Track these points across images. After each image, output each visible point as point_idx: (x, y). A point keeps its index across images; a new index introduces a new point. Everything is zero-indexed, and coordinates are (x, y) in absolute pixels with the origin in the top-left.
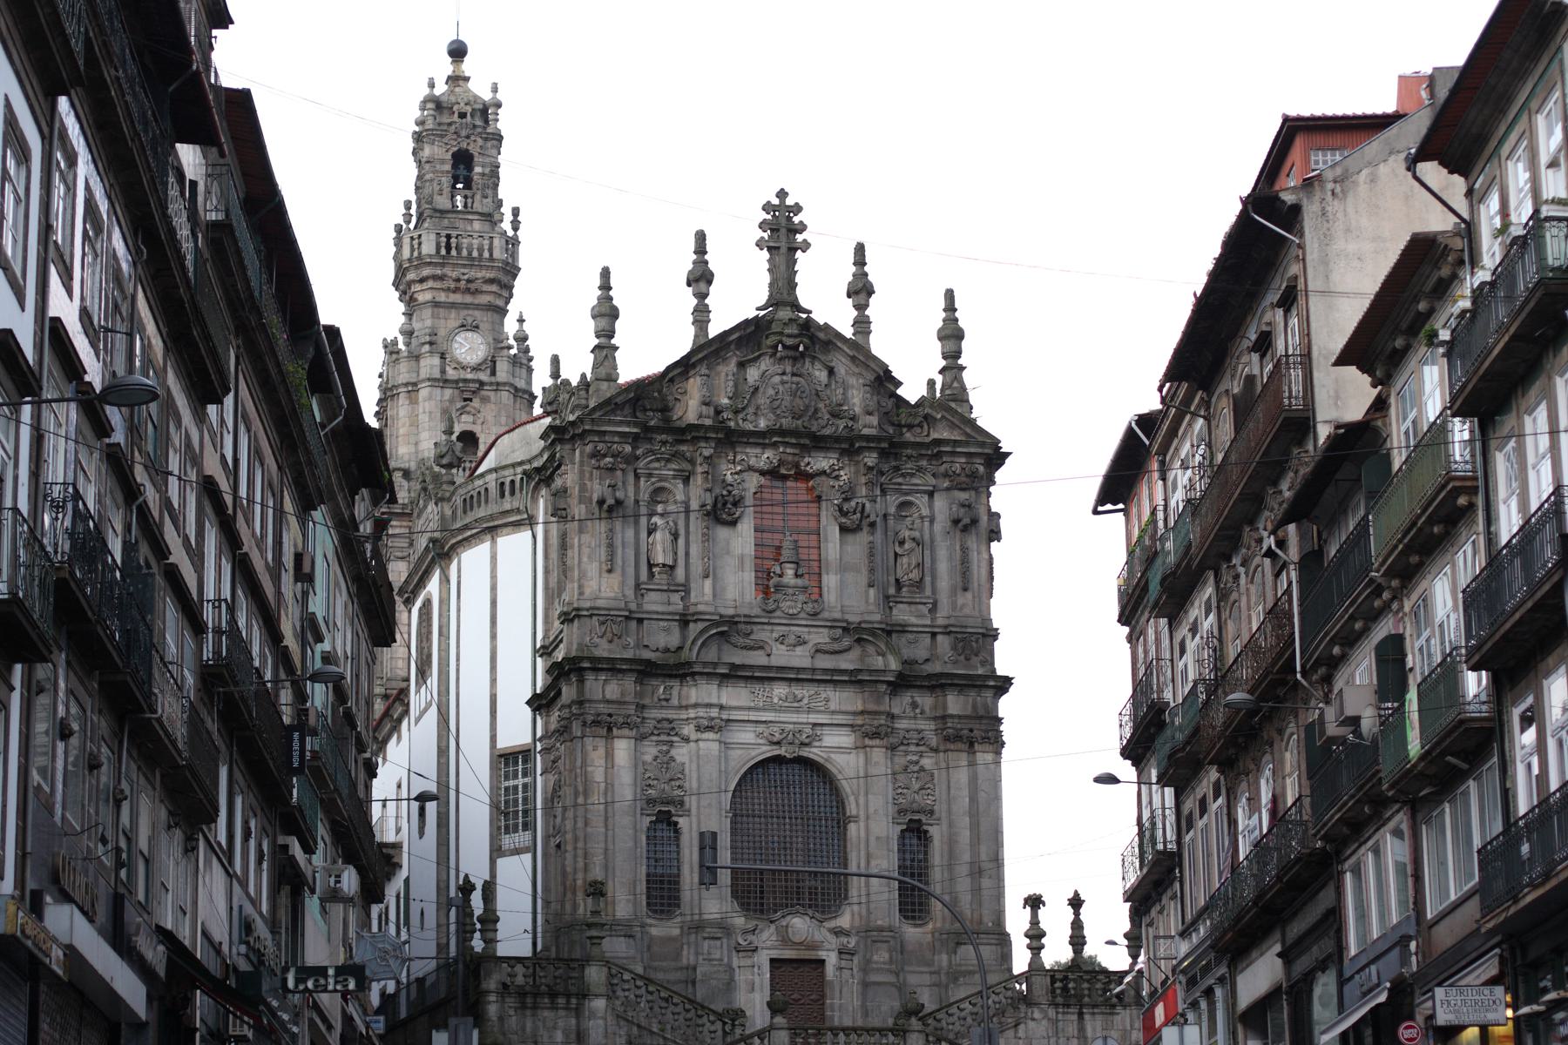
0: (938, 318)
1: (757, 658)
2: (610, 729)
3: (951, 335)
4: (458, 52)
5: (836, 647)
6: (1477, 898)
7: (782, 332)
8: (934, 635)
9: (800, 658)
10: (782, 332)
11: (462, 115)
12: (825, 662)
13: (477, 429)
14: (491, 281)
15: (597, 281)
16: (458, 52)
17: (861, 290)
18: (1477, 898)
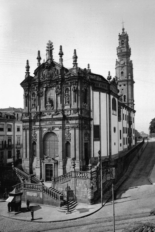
0: (73, 55)
1: (45, 117)
2: (26, 130)
3: (76, 58)
4: (123, 29)
5: (55, 114)
6: (122, 197)
7: (50, 65)
8: (71, 110)
9: (50, 117)
10: (50, 65)
11: (123, 36)
12: (54, 117)
13: (123, 71)
14: (126, 54)
15: (26, 62)
16: (123, 29)
17: (61, 54)
18: (122, 197)
